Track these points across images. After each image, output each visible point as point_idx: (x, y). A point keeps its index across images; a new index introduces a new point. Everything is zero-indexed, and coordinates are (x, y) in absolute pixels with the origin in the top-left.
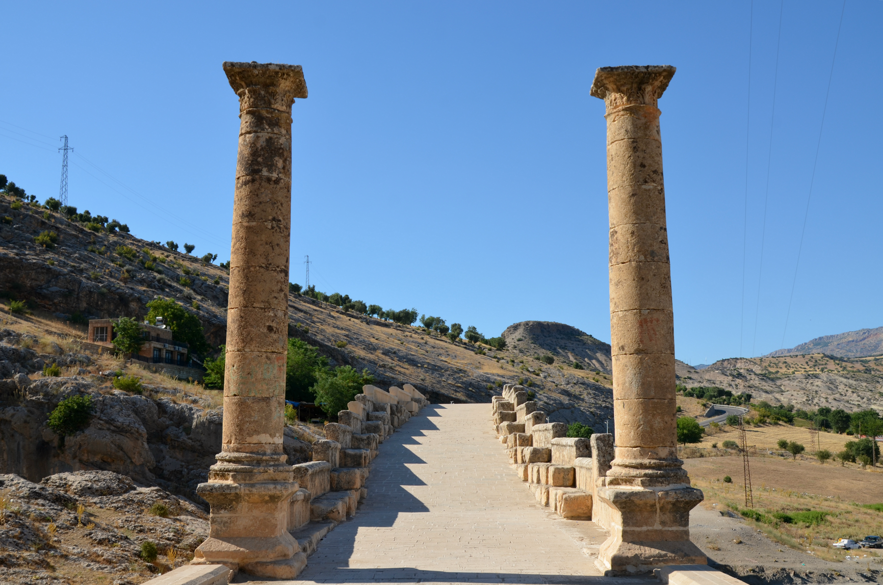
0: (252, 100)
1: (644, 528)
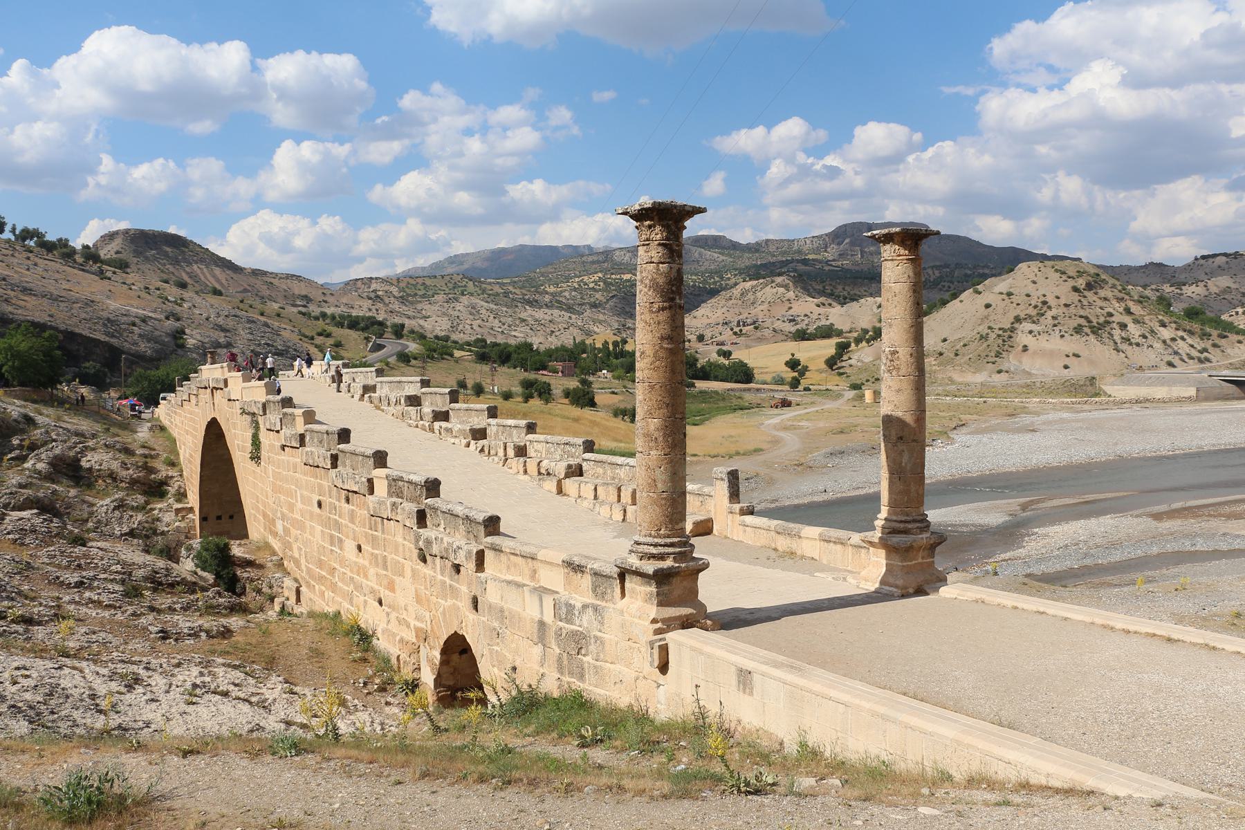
0: (664, 234)
1: (914, 562)
